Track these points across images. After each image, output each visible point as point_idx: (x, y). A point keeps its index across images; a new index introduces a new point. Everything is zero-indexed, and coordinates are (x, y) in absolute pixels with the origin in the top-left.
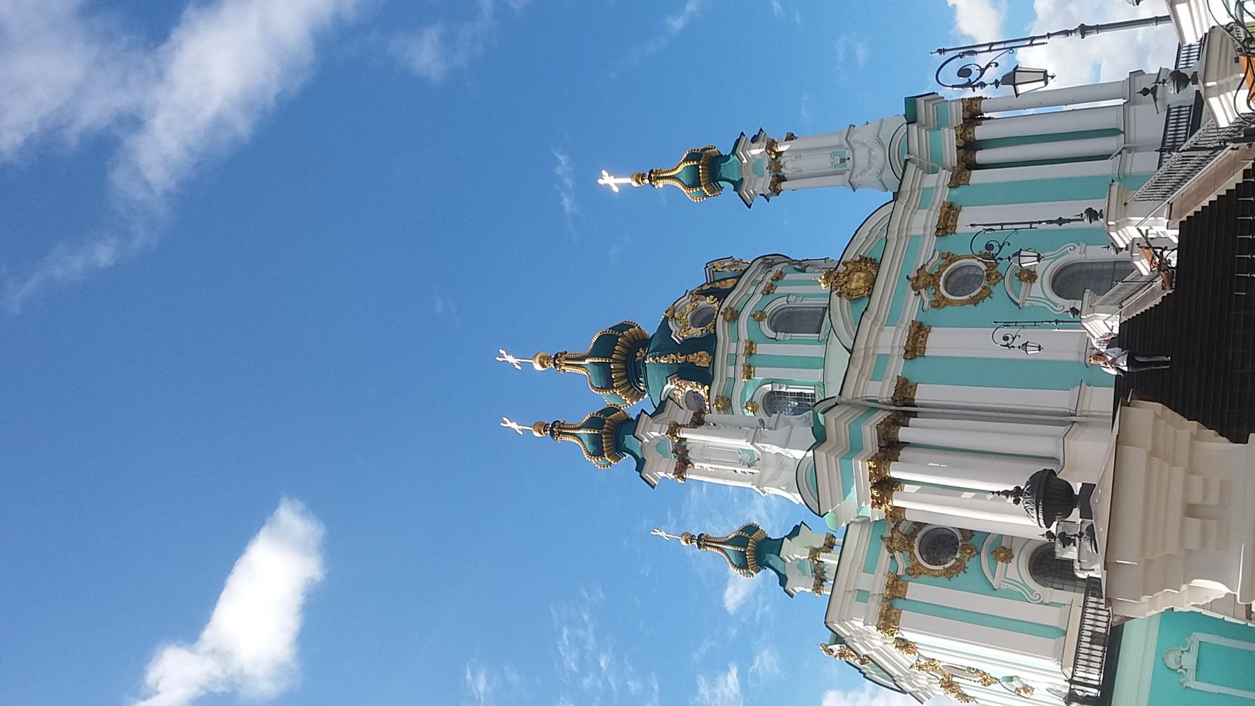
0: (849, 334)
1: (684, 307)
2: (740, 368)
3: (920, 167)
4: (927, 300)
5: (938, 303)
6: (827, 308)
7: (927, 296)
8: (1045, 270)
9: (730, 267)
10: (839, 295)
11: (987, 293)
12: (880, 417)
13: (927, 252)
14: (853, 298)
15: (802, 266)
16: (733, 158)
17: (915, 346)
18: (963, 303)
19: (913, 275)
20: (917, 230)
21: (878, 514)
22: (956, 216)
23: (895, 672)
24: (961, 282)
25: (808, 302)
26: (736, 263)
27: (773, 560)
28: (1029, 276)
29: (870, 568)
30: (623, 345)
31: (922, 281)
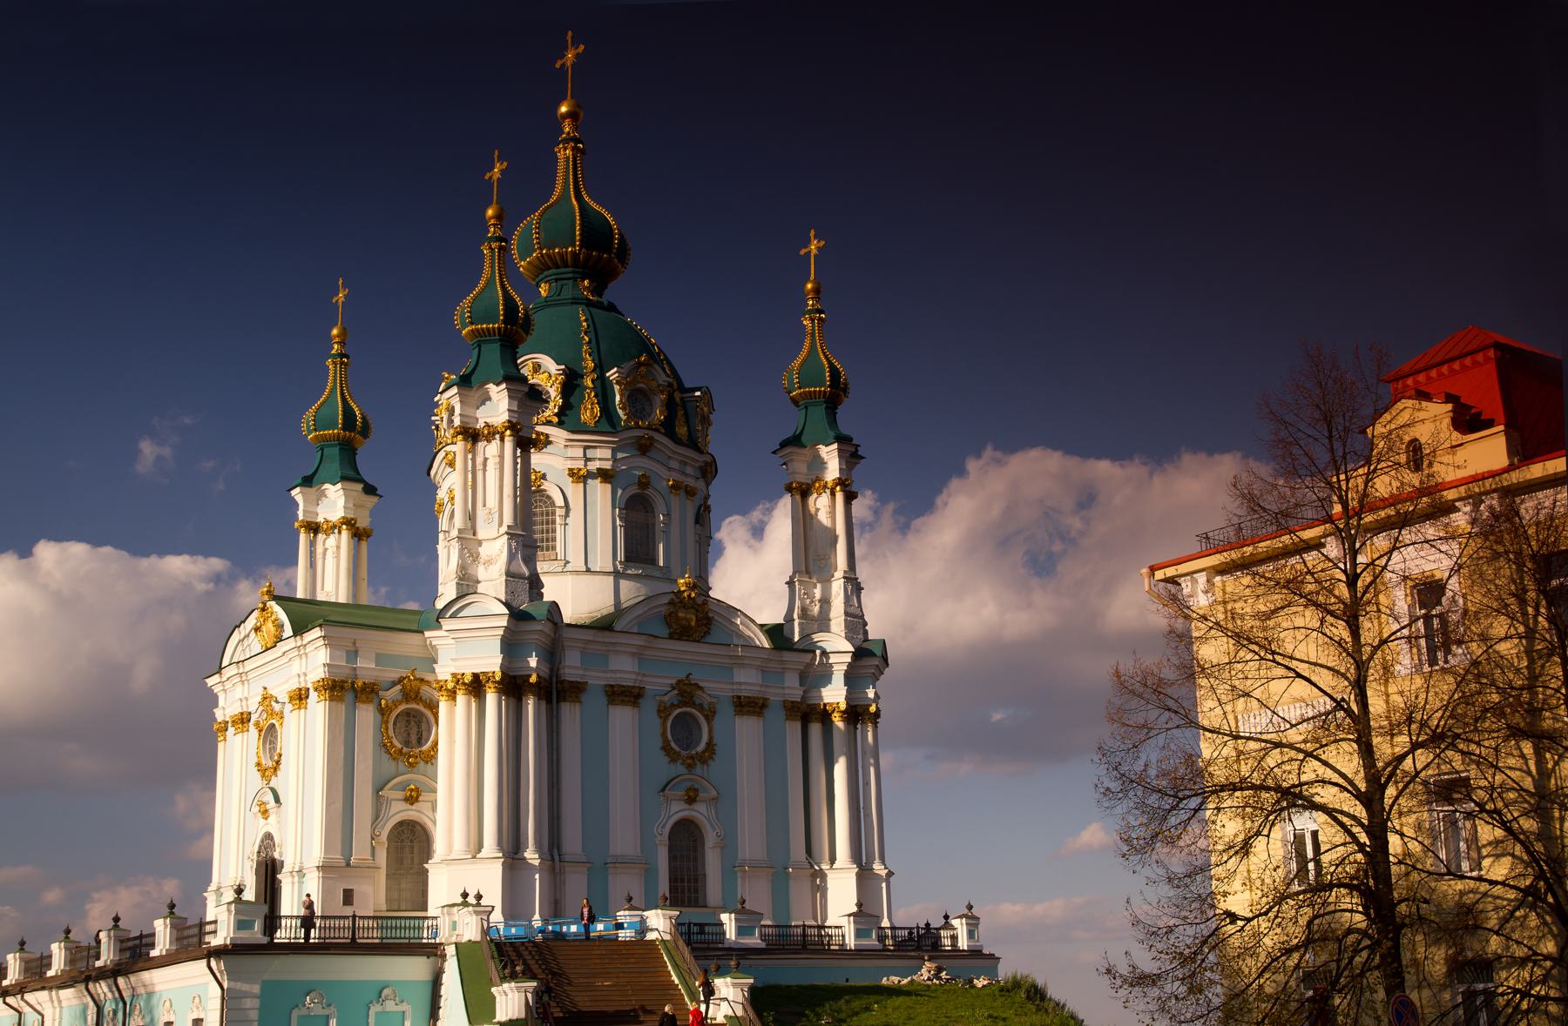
2: (580, 464)
4: (666, 698)
5: (663, 711)
7: (672, 697)
8: (700, 812)
10: (671, 603)
11: (673, 756)
14: (669, 619)
16: (832, 434)
19: (695, 678)
23: (249, 665)
24: (684, 730)
26: (706, 421)
28: (691, 799)
29: (380, 659)
31: (686, 691)
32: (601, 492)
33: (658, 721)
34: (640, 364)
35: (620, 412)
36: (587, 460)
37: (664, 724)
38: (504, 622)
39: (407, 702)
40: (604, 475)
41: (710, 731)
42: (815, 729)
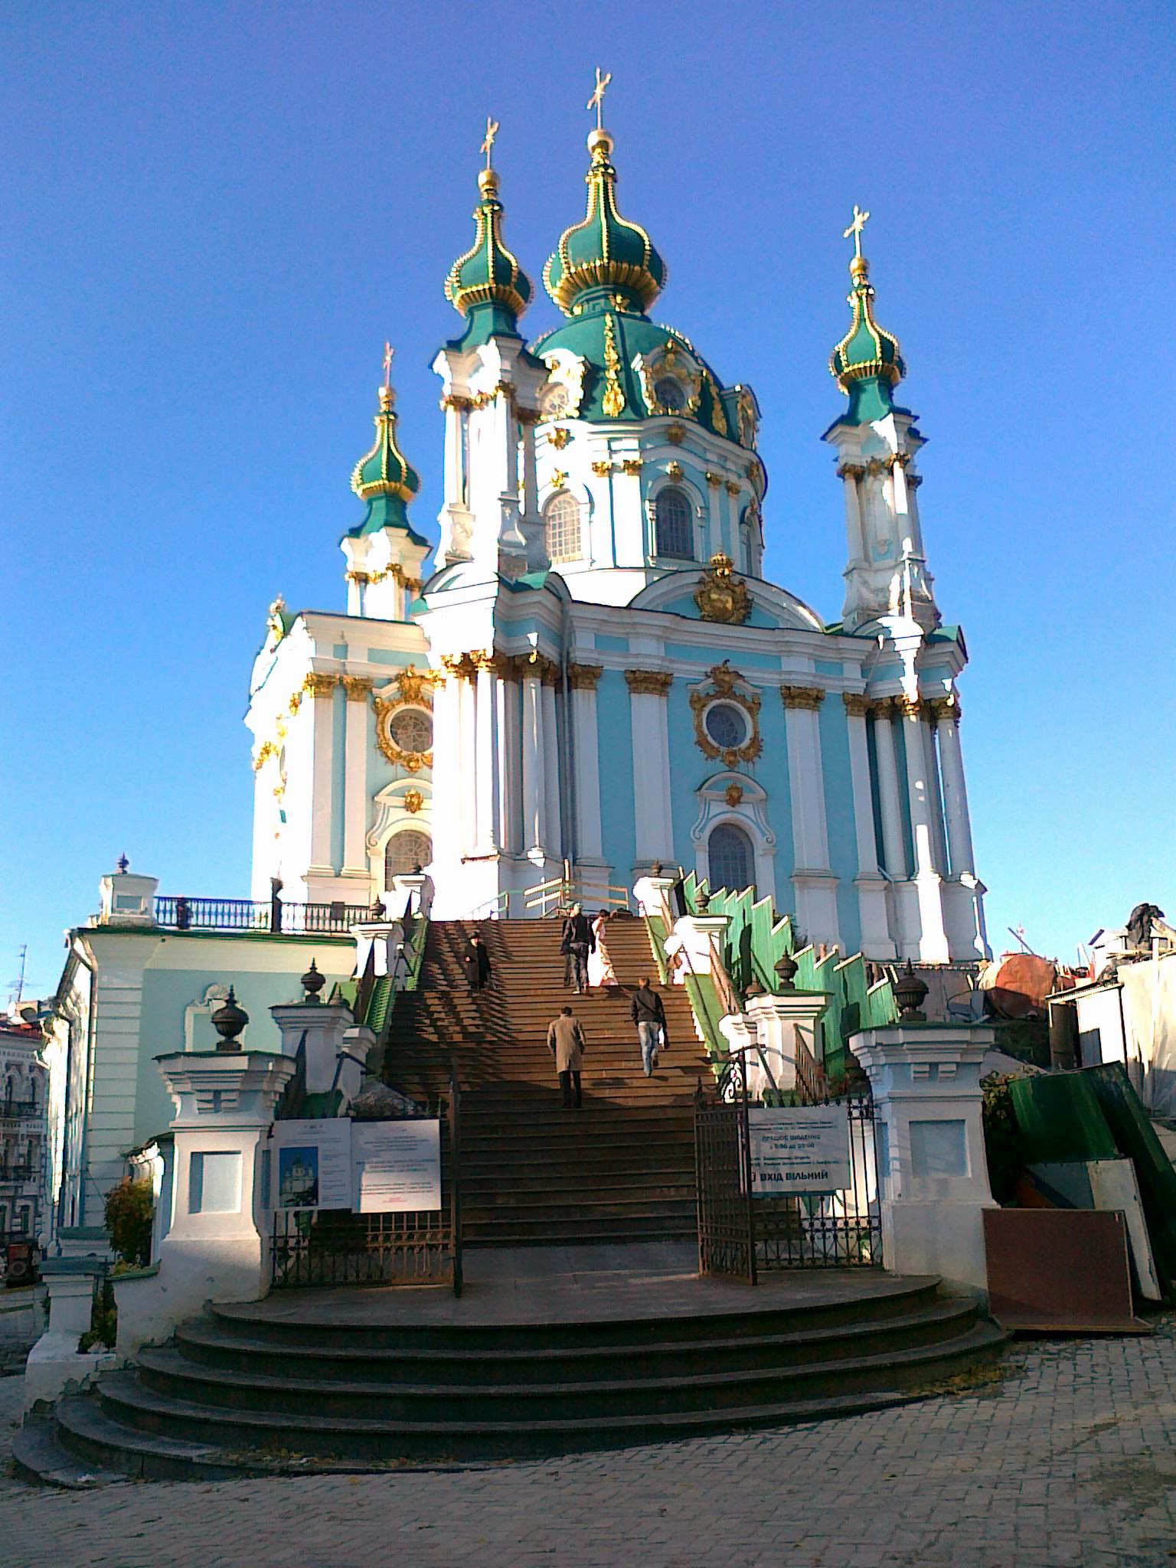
0: (649, 602)
1: (684, 366)
3: (871, 655)
4: (699, 687)
6: (692, 559)
8: (746, 815)
9: (746, 419)
10: (701, 582)
11: (711, 754)
12: (551, 653)
13: (761, 678)
14: (699, 599)
15: (750, 519)
16: (885, 408)
17: (642, 681)
18: (699, 728)
20: (789, 664)
21: (436, 664)
22: (807, 706)
25: (698, 535)
26: (751, 424)
27: (380, 515)
28: (734, 801)
30: (631, 271)
31: (724, 680)
32: (628, 485)
33: (692, 713)
34: (667, 351)
35: (648, 403)
36: (612, 452)
37: (699, 715)
38: (493, 589)
39: (407, 702)
40: (631, 467)
41: (755, 727)
42: (883, 726)
